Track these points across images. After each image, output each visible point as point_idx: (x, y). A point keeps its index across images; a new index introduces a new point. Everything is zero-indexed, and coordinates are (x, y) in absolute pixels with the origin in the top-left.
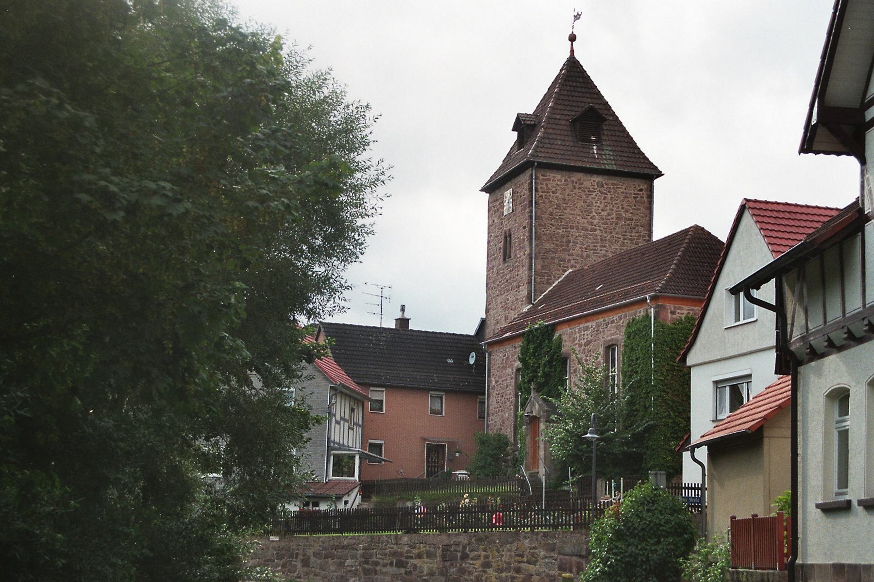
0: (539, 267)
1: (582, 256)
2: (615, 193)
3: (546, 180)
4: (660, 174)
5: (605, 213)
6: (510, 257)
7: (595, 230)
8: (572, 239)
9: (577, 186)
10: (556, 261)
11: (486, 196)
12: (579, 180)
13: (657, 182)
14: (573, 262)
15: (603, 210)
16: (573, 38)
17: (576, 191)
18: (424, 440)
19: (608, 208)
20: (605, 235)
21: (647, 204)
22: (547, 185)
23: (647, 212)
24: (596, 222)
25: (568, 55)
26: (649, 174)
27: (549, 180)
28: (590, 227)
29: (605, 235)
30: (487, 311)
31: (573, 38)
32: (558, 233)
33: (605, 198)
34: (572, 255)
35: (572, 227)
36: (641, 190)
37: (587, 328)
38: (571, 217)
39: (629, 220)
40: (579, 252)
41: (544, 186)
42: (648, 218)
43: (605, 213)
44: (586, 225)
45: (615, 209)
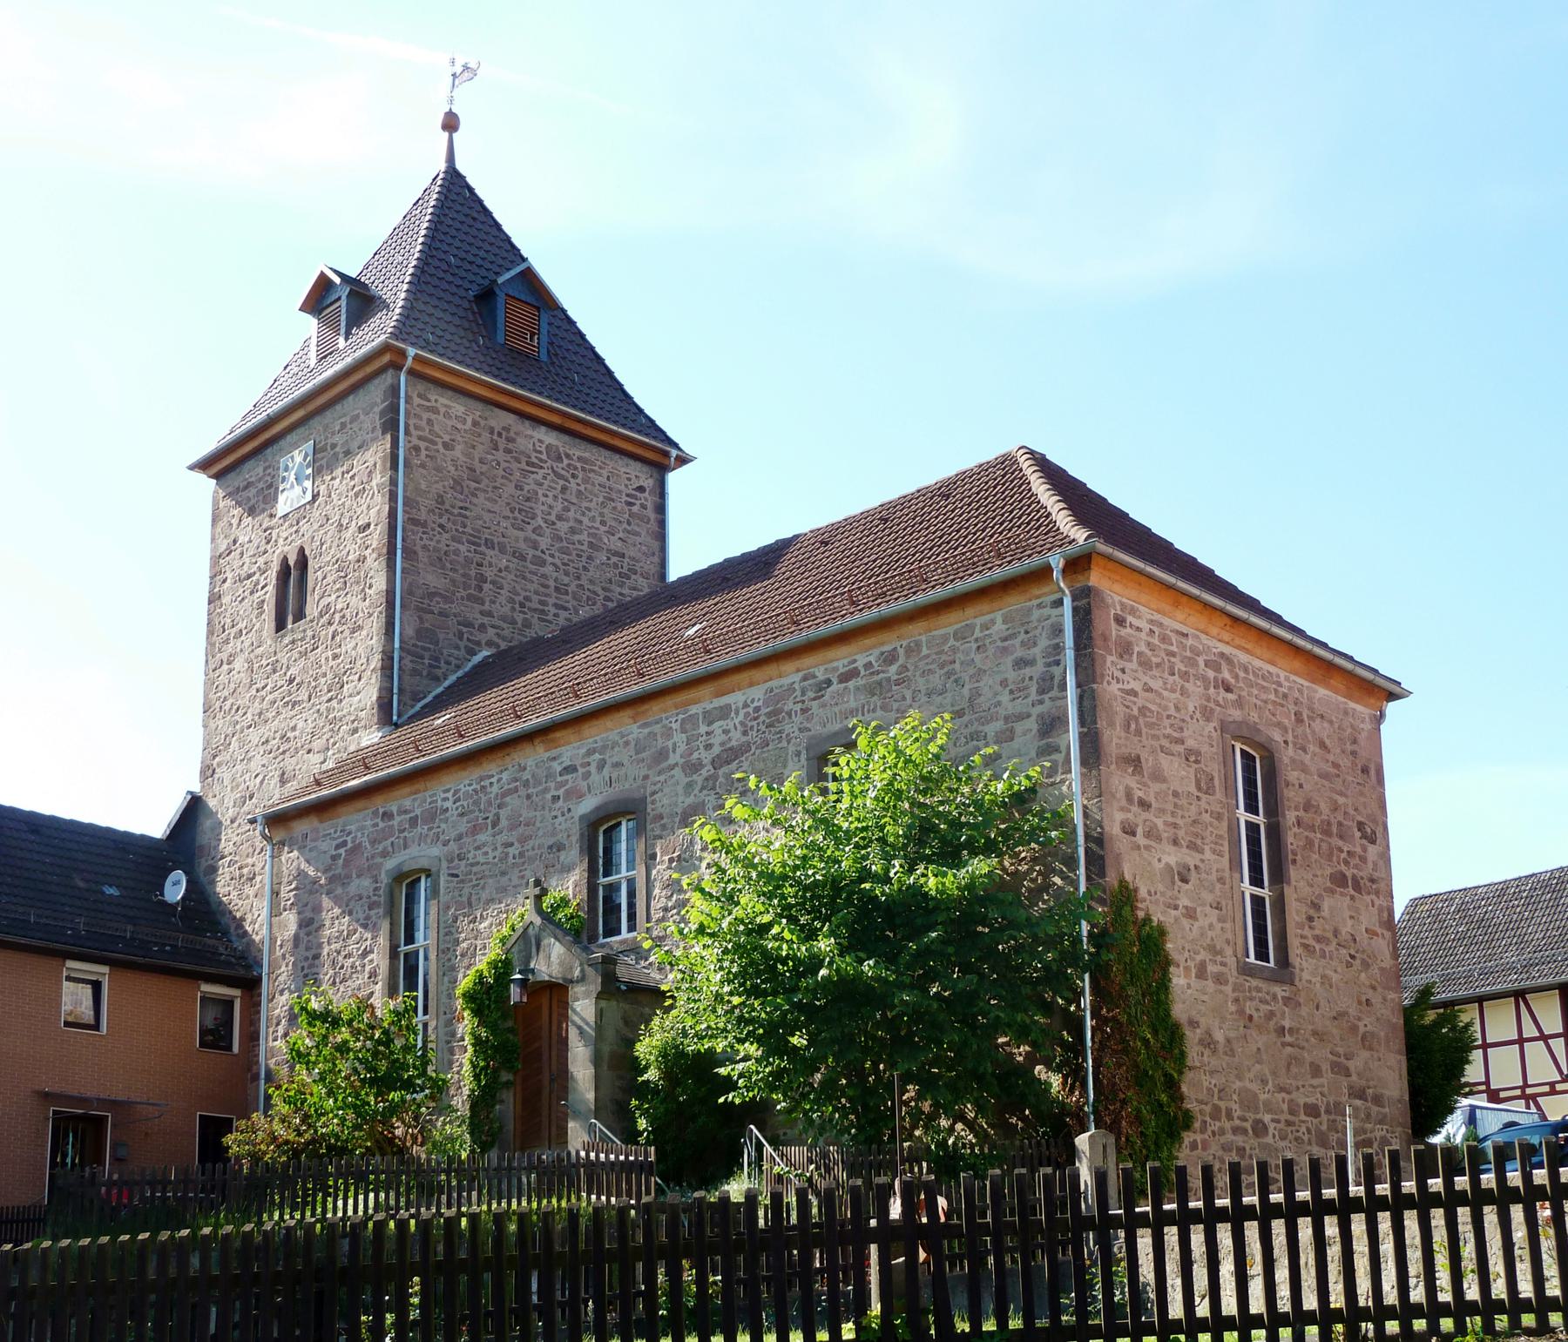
0: (410, 632)
1: (513, 622)
2: (586, 481)
3: (429, 409)
4: (683, 460)
5: (563, 527)
6: (300, 615)
7: (543, 563)
8: (489, 573)
9: (502, 443)
10: (452, 622)
11: (206, 485)
12: (507, 429)
13: (674, 479)
14: (491, 631)
15: (559, 518)
16: (451, 124)
17: (500, 455)
18: (47, 1097)
19: (571, 514)
20: (566, 580)
21: (653, 526)
22: (429, 421)
23: (656, 545)
24: (544, 542)
25: (443, 166)
26: (658, 455)
27: (435, 411)
28: (531, 552)
29: (566, 580)
30: (207, 772)
31: (451, 124)
32: (457, 552)
33: (564, 489)
34: (490, 614)
35: (489, 544)
36: (641, 489)
37: (724, 713)
38: (487, 517)
39: (616, 554)
40: (506, 610)
41: (423, 424)
42: (656, 559)
43: (563, 527)
44: (522, 545)
45: (585, 520)
